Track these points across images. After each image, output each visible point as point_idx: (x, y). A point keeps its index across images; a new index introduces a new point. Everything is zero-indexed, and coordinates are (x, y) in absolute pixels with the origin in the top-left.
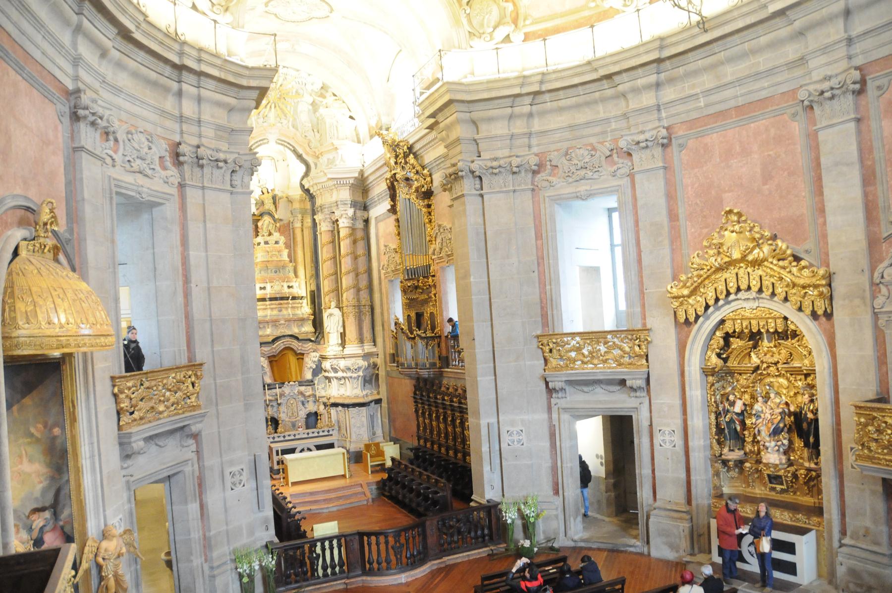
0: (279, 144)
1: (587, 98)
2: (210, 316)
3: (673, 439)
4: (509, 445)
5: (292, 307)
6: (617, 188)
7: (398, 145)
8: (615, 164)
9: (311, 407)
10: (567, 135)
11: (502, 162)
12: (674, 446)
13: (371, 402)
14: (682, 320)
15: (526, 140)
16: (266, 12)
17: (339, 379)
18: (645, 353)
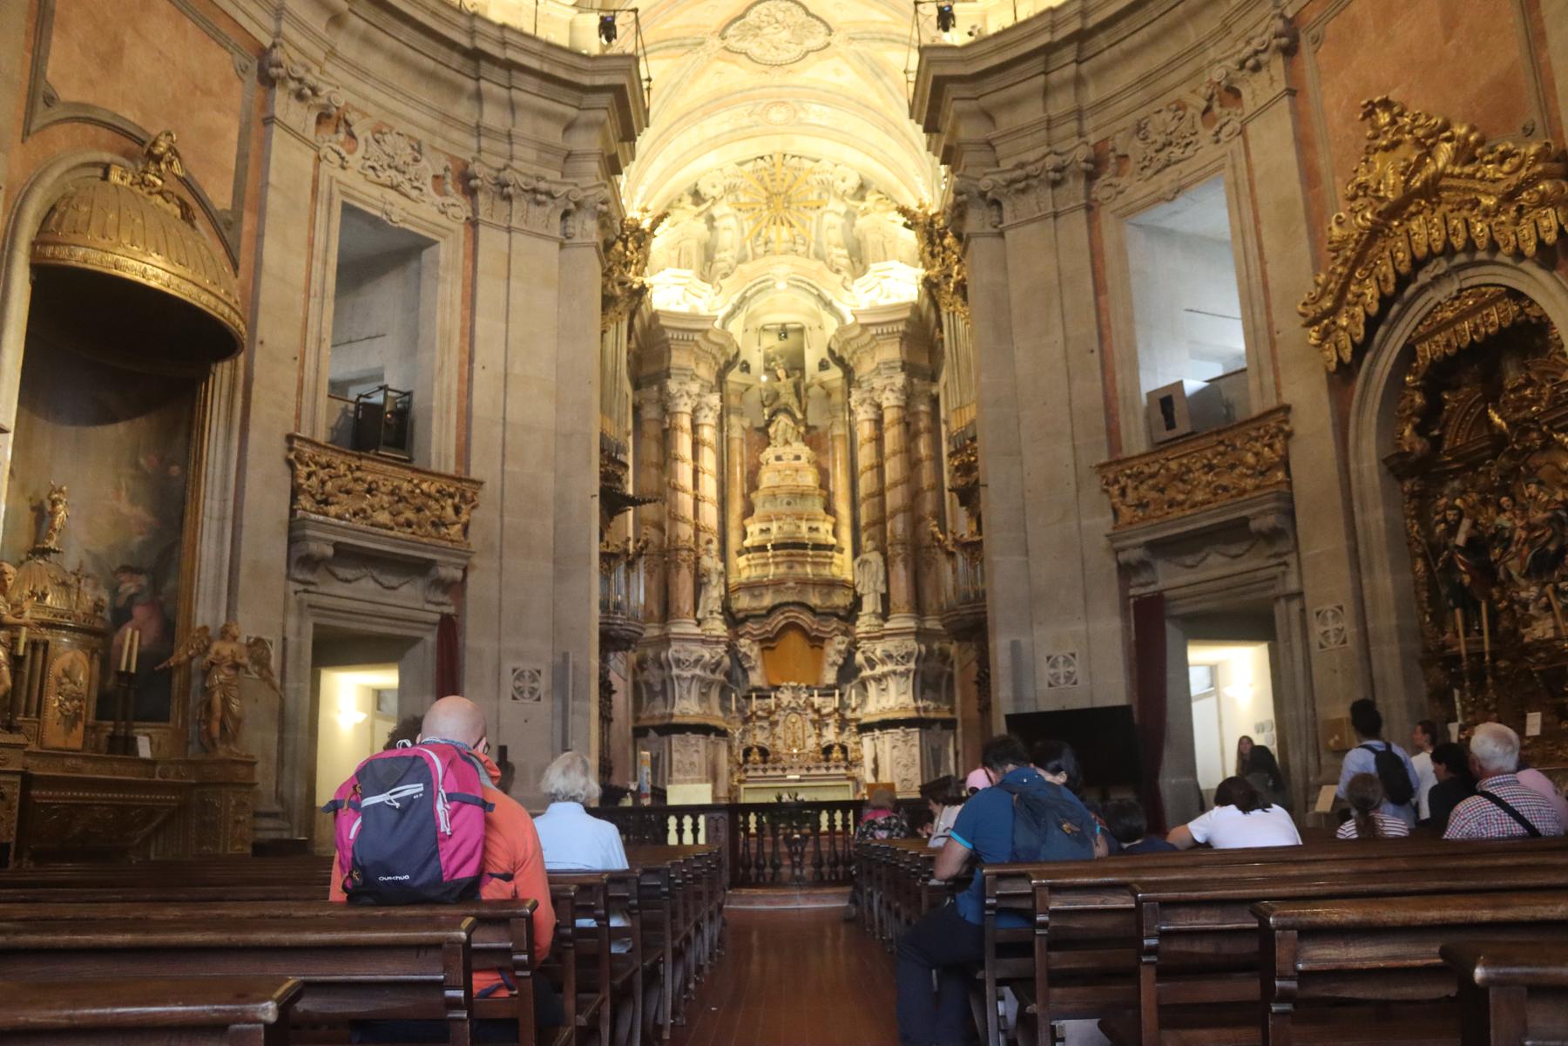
0: (793, 286)
1: (1167, 19)
2: (504, 419)
3: (1340, 626)
4: (1050, 685)
5: (815, 564)
6: (1220, 162)
7: (932, 224)
8: (1215, 120)
9: (830, 735)
10: (1140, 96)
11: (1030, 169)
12: (1344, 642)
13: (934, 721)
14: (1333, 366)
15: (1074, 125)
16: (726, 48)
17: (878, 679)
18: (1281, 457)
